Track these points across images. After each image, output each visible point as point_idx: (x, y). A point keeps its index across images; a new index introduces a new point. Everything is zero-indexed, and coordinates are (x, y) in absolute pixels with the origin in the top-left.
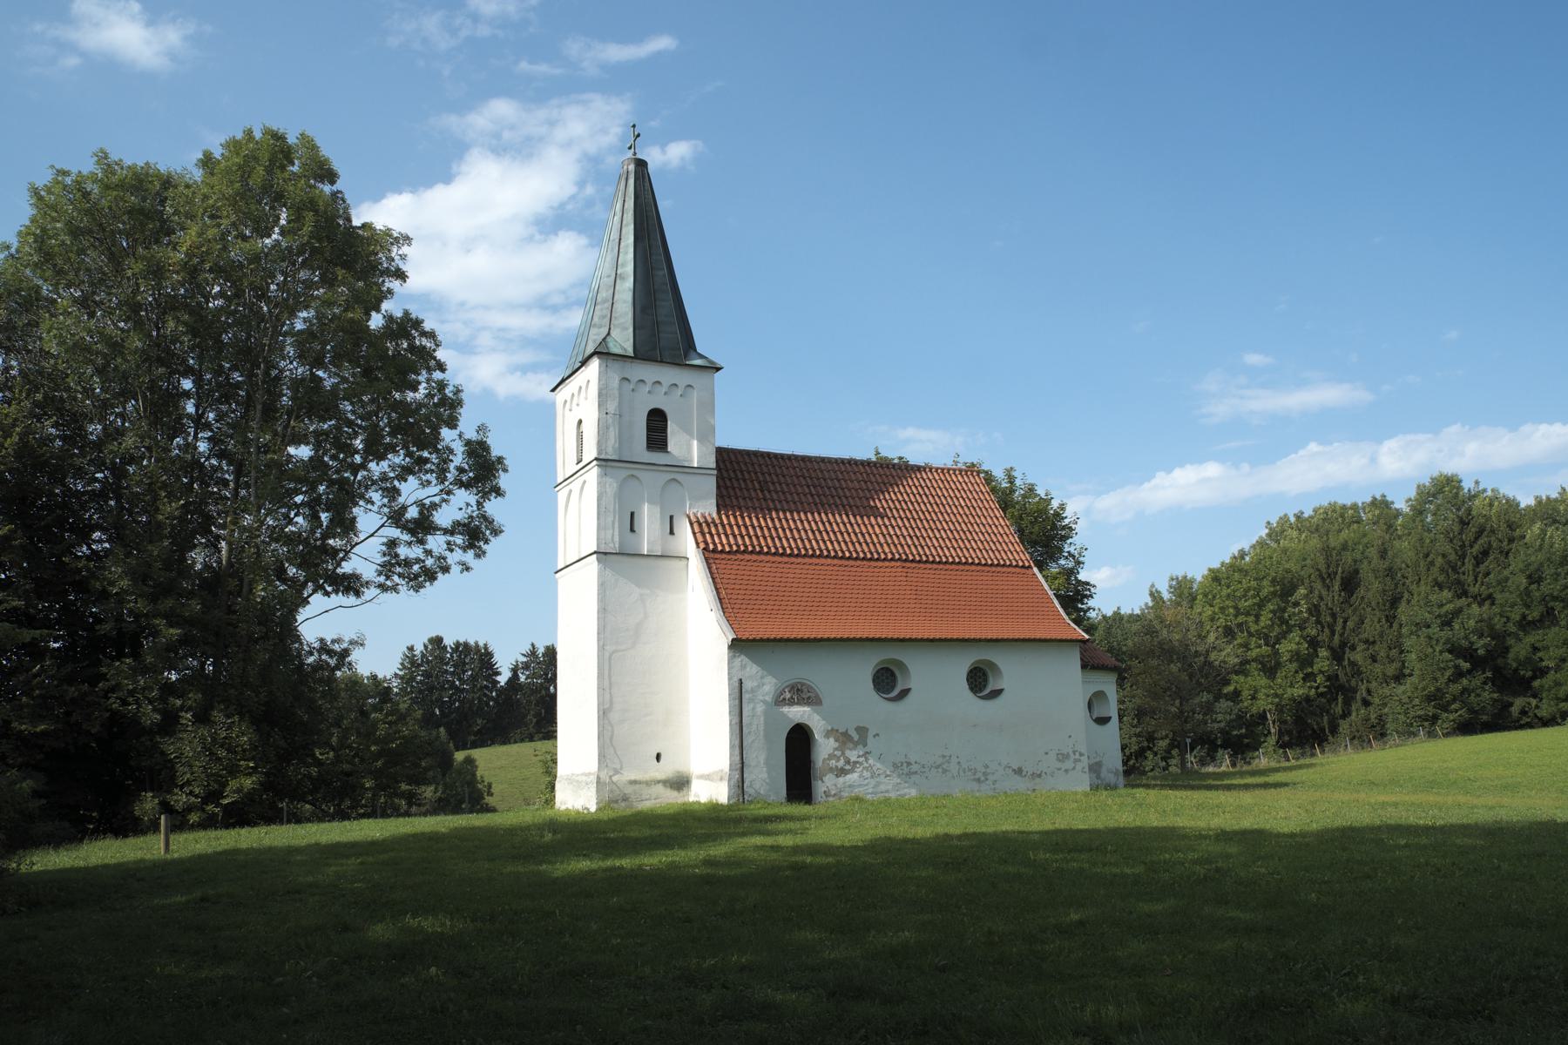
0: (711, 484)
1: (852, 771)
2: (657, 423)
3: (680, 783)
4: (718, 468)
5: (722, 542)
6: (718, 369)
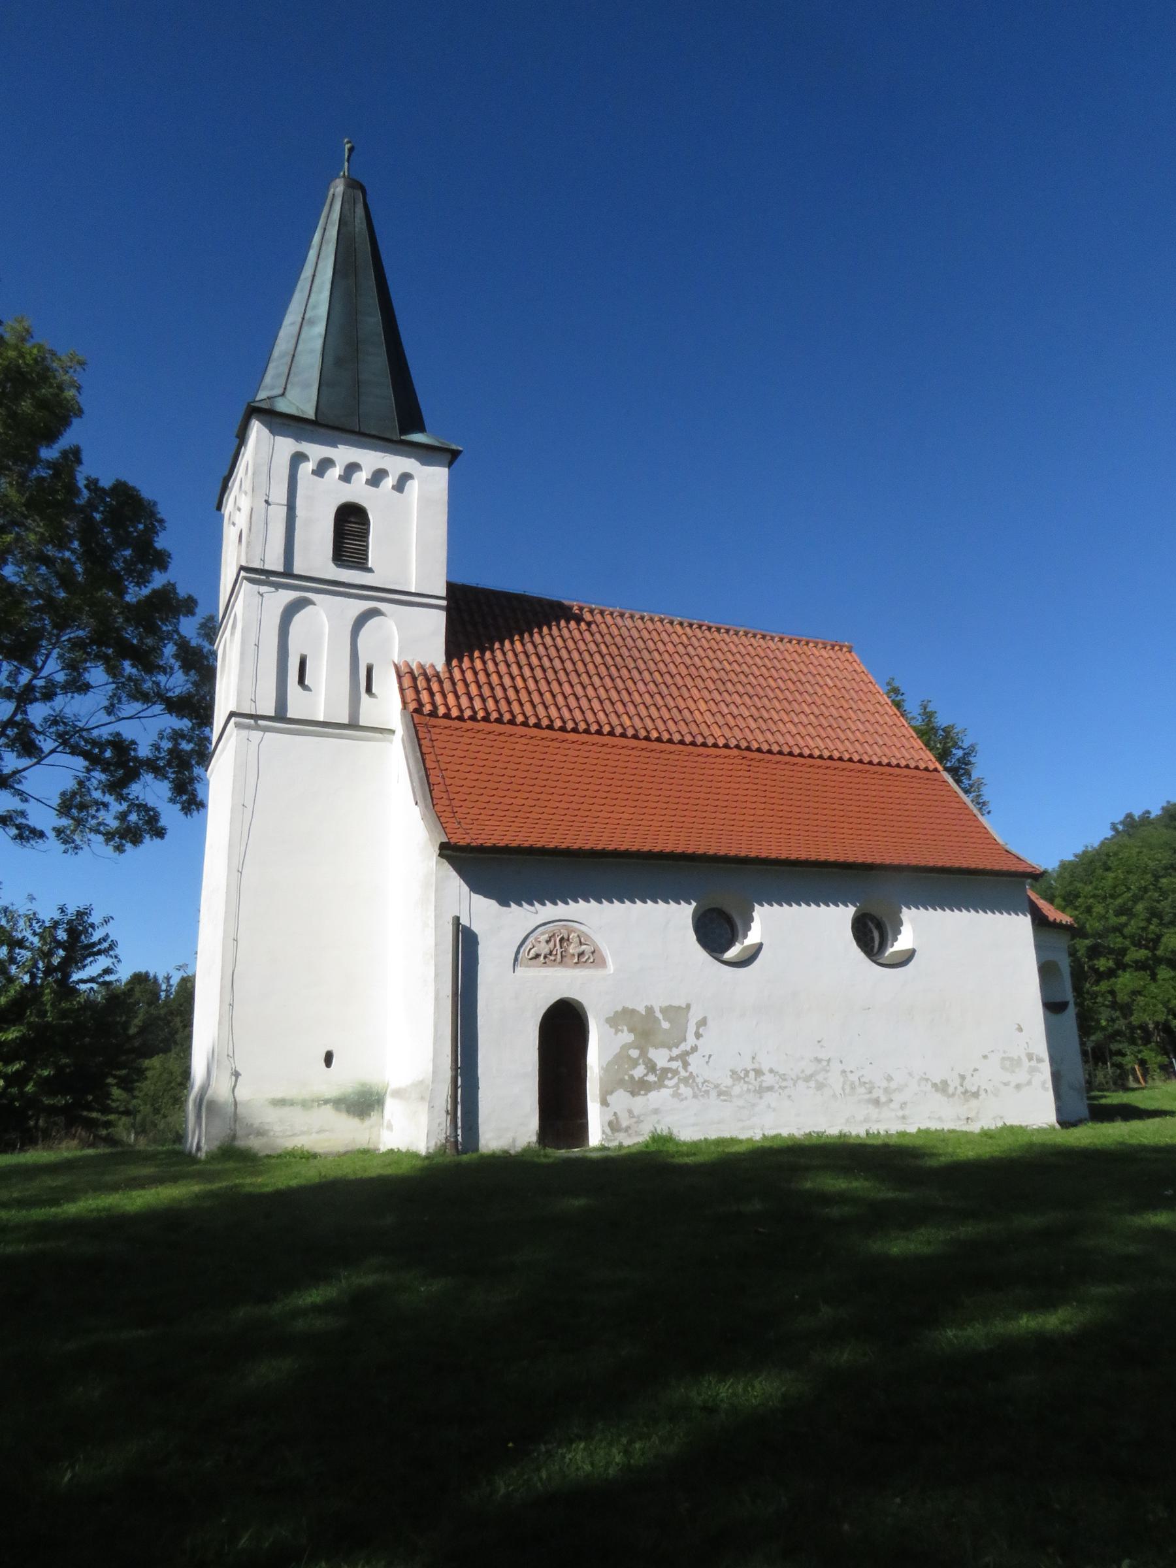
1: (660, 1085)
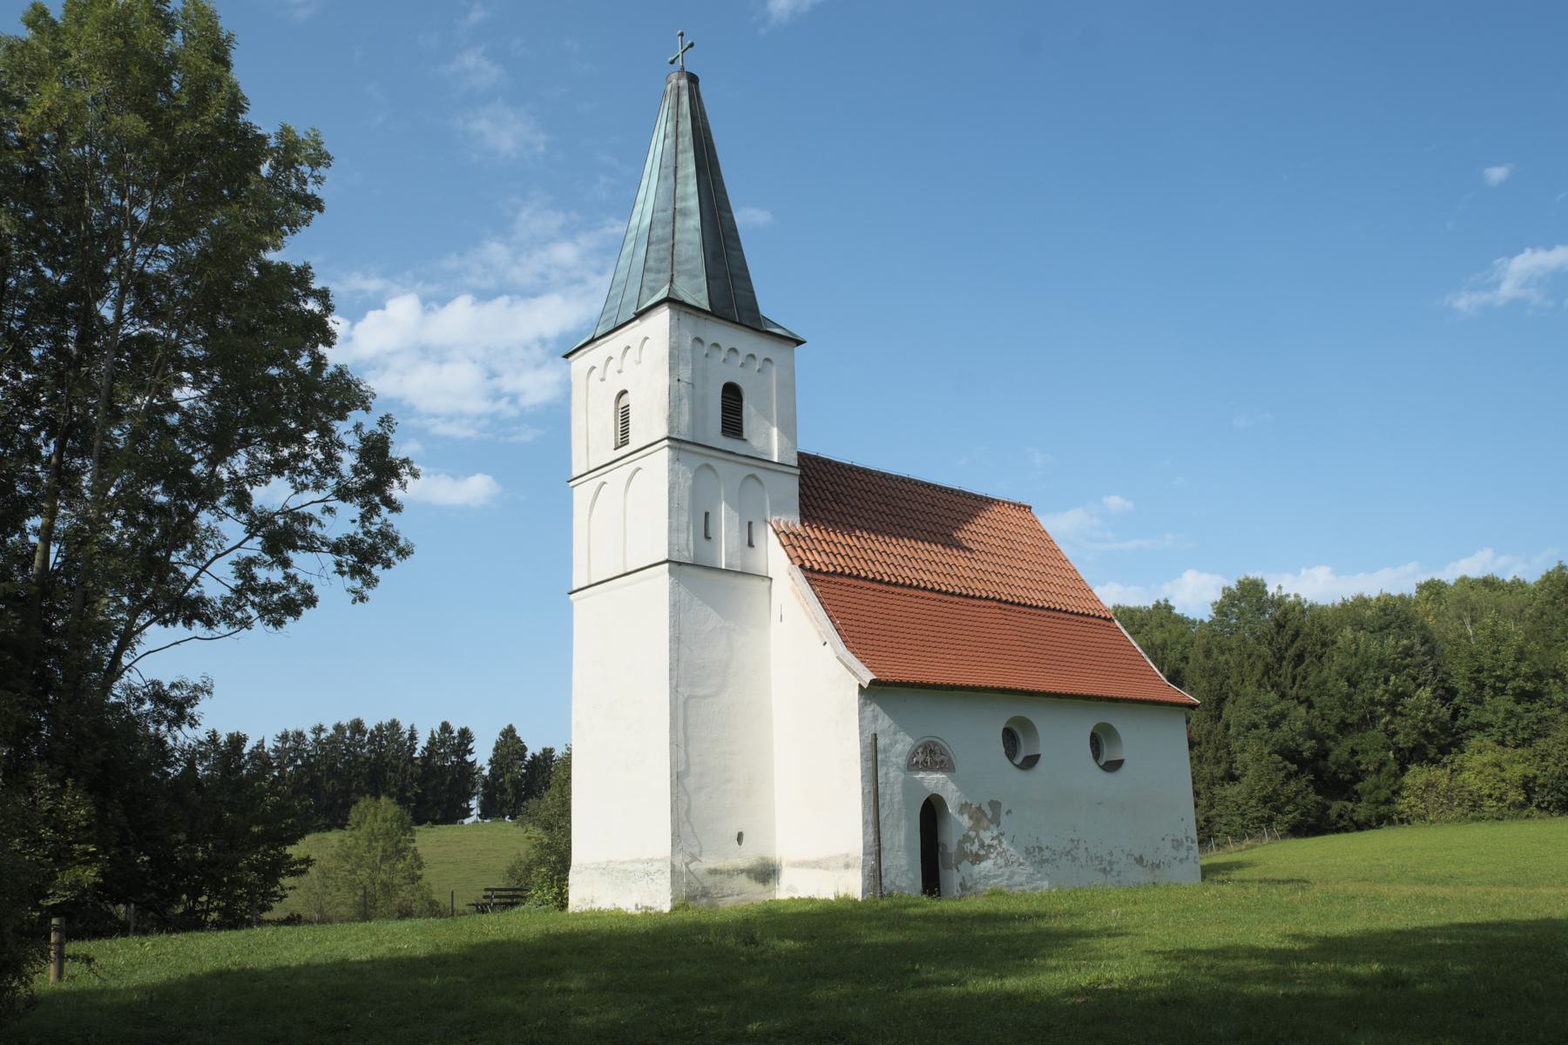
0: (791, 487)
1: (986, 857)
2: (732, 396)
3: (766, 873)
4: (800, 466)
5: (816, 560)
6: (799, 342)
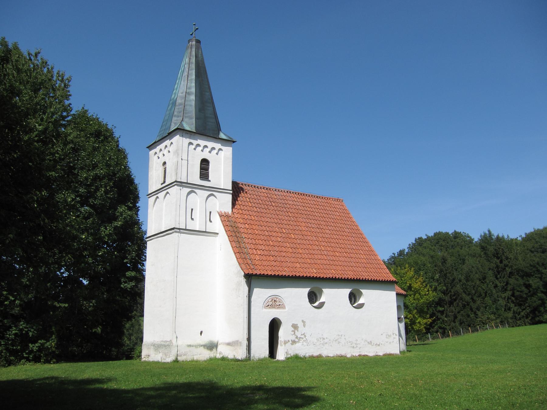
1: (299, 342)
4: (233, 190)
